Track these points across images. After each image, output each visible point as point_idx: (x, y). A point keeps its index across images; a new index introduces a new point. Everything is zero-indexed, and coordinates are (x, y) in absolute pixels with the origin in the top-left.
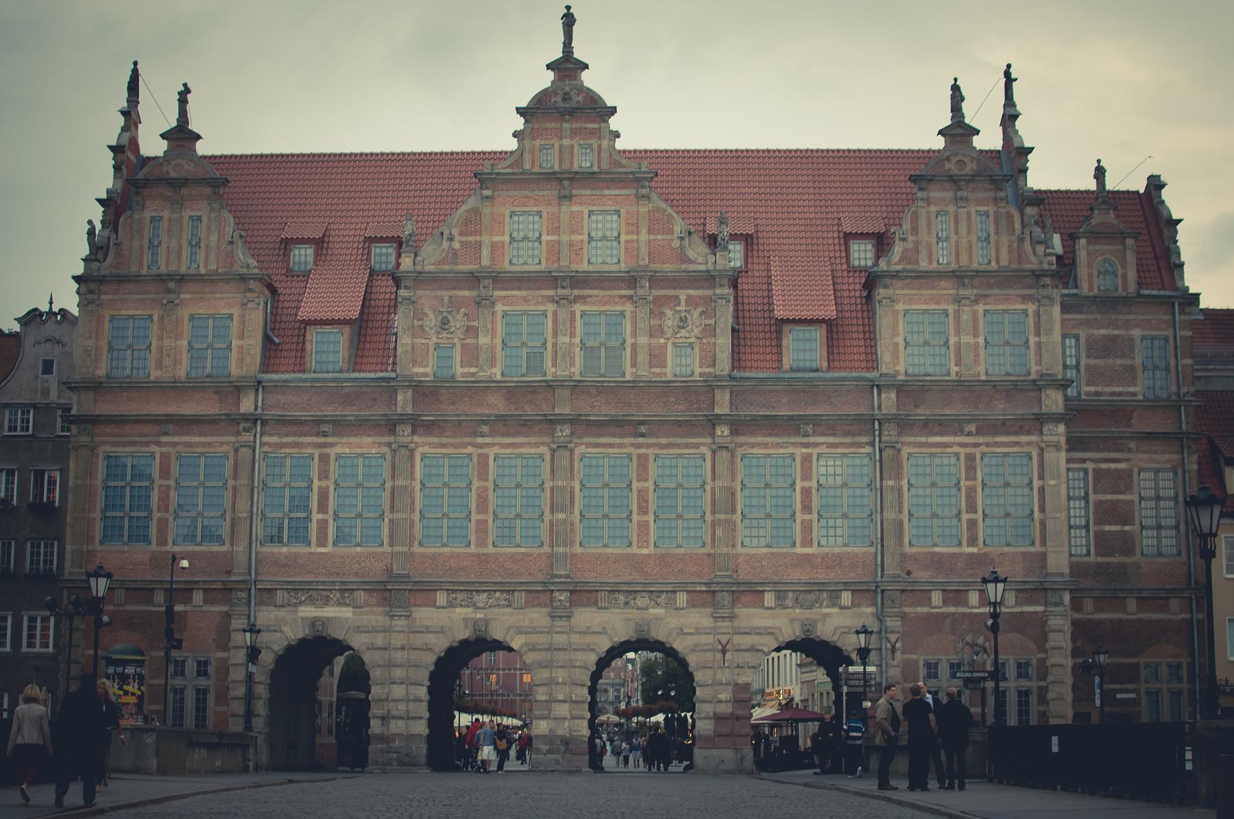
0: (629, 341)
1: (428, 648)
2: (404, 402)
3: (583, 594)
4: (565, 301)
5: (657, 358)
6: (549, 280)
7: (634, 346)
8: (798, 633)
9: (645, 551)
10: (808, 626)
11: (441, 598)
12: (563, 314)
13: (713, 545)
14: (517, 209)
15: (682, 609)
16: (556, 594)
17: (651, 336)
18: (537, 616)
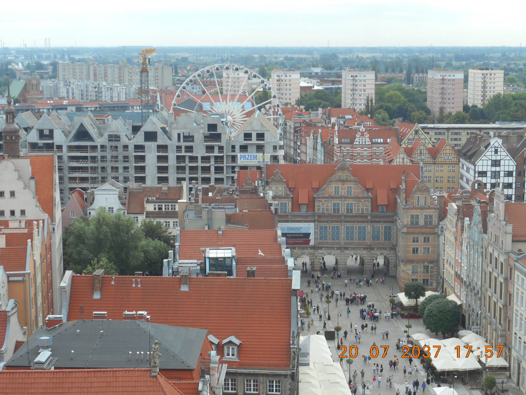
0: (354, 208)
3: (346, 248)
6: (341, 198)
11: (323, 249)
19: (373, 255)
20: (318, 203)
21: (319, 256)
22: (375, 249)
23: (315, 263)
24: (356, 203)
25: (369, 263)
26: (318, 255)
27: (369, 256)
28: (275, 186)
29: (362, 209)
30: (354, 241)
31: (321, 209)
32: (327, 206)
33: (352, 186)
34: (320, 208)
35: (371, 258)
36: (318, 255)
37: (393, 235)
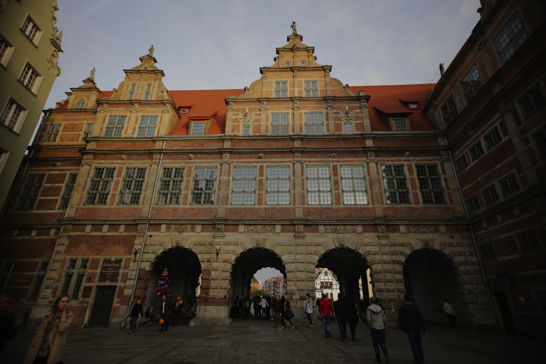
1: (233, 252)
2: (227, 145)
4: (297, 109)
5: (338, 127)
6: (292, 99)
7: (328, 125)
8: (422, 247)
9: (339, 206)
10: (426, 243)
11: (241, 228)
12: (297, 112)
13: (373, 204)
14: (278, 80)
15: (361, 233)
16: (297, 226)
17: (335, 121)
18: (287, 237)
19: (400, 249)
20: (234, 115)
21: (227, 252)
22: (402, 229)
23: (213, 274)
24: (330, 111)
25: (389, 276)
26: (224, 248)
27: (387, 249)
28: (138, 82)
29: (345, 123)
30: (334, 206)
31: (241, 128)
32: (258, 120)
33: (318, 79)
34: (238, 126)
35: (394, 258)
36: (224, 248)
37: (448, 187)
